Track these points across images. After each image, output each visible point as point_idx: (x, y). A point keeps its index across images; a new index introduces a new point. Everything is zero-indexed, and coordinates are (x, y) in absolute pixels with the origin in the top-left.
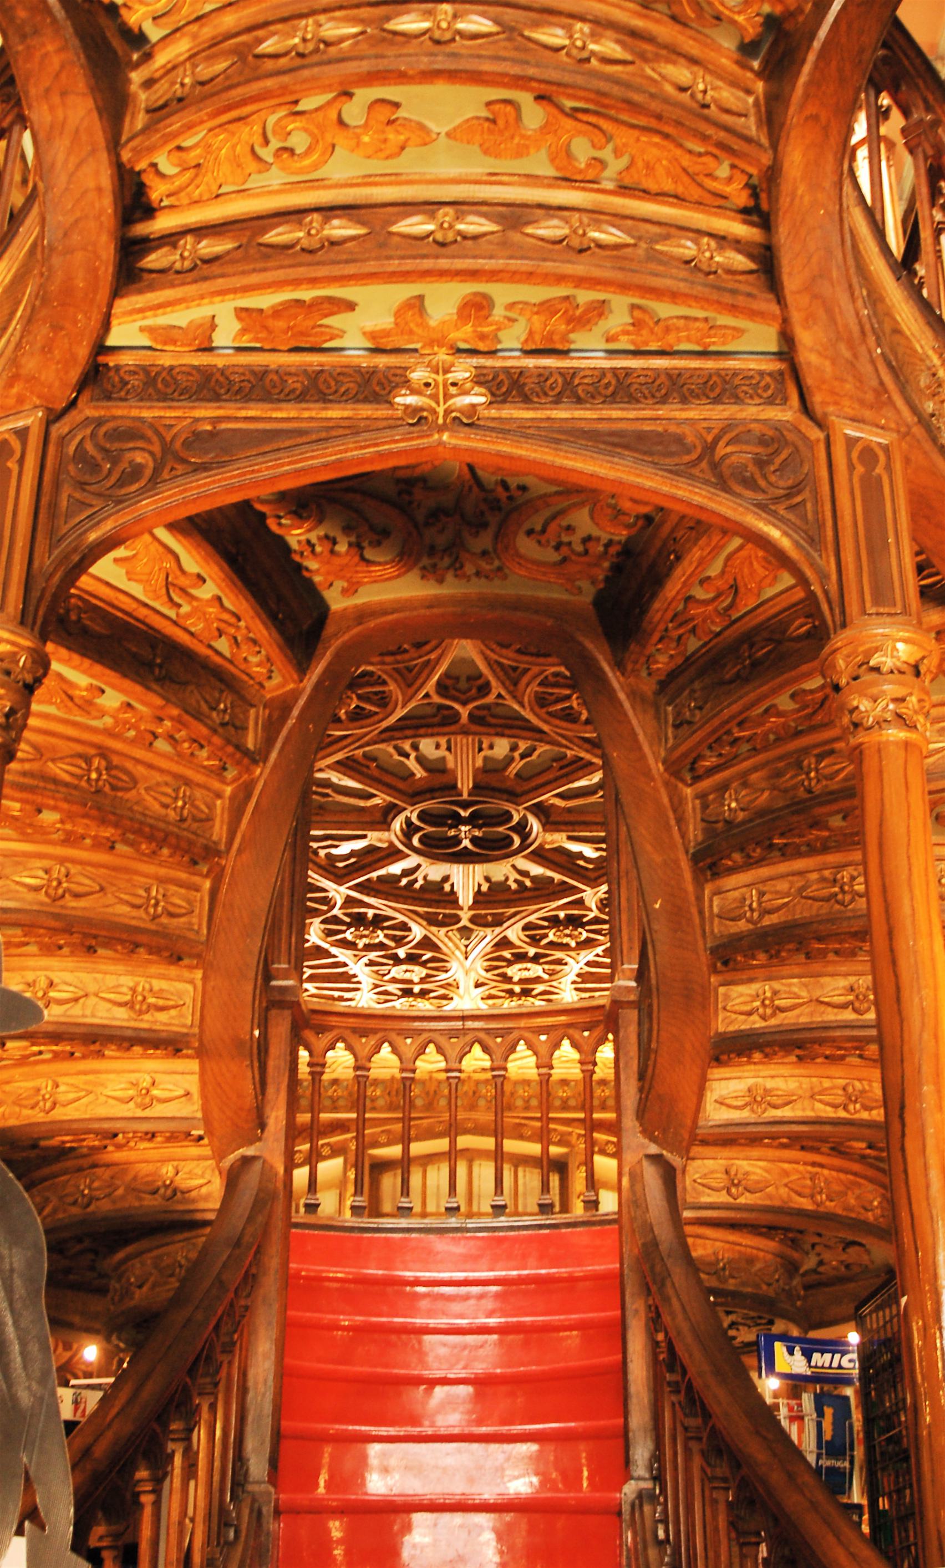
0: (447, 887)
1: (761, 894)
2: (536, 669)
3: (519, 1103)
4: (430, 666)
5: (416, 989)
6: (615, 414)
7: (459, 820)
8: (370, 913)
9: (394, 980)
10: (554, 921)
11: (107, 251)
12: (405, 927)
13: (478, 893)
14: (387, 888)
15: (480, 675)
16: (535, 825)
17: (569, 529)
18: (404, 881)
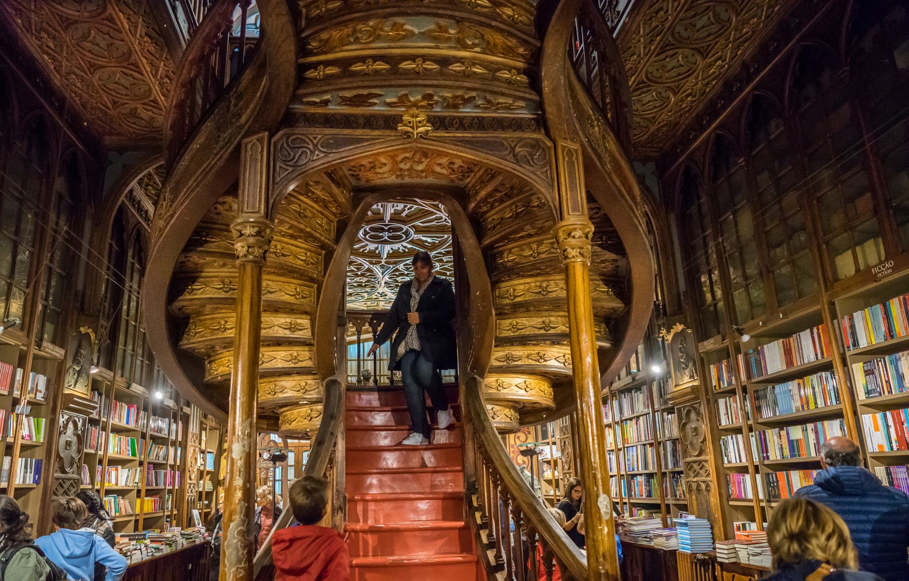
0: (377, 252)
1: (515, 290)
6: (478, 135)
7: (382, 230)
9: (356, 282)
11: (292, 70)
13: (388, 253)
16: (412, 231)
18: (362, 250)
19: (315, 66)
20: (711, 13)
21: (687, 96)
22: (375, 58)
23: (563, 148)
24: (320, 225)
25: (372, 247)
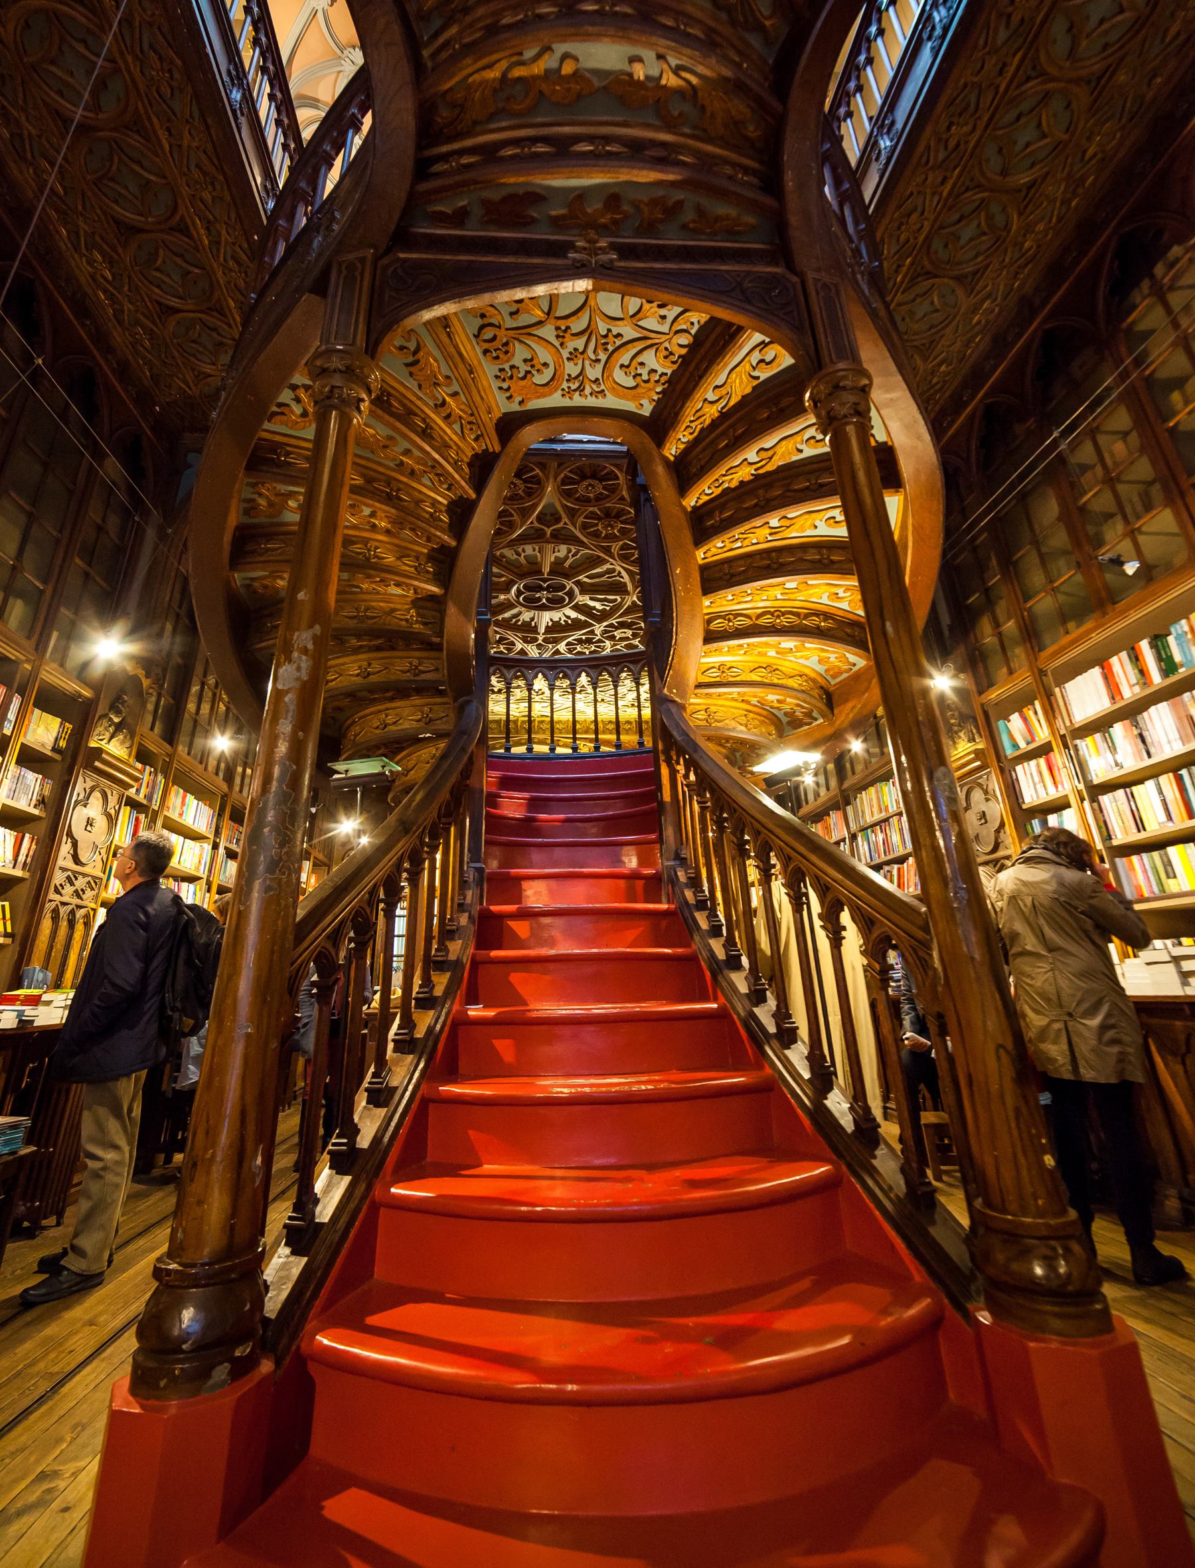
2: (583, 508)
7: (541, 589)
10: (580, 641)
12: (513, 644)
13: (547, 627)
15: (558, 512)
16: (577, 591)
17: (642, 364)
19: (445, 157)
20: (983, 213)
21: (940, 365)
25: (526, 616)
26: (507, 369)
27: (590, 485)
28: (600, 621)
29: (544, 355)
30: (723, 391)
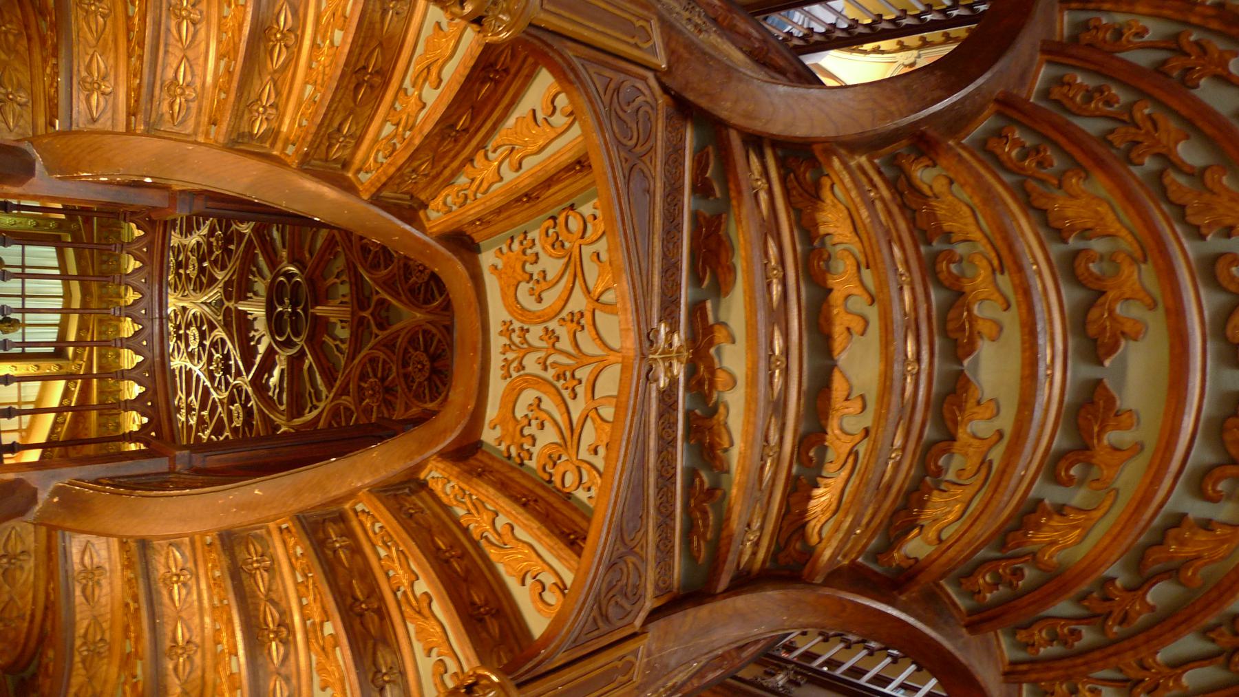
0: (250, 295)
2: (394, 358)
3: (104, 328)
4: (397, 295)
5: (181, 271)
7: (294, 304)
8: (232, 247)
9: (187, 259)
10: (227, 357)
12: (223, 268)
13: (246, 313)
14: (249, 259)
15: (390, 325)
17: (542, 426)
18: (254, 269)
22: (784, 282)
23: (635, 653)
24: (414, 171)
26: (535, 250)
27: (424, 366)
28: (253, 383)
29: (551, 297)
30: (507, 538)
